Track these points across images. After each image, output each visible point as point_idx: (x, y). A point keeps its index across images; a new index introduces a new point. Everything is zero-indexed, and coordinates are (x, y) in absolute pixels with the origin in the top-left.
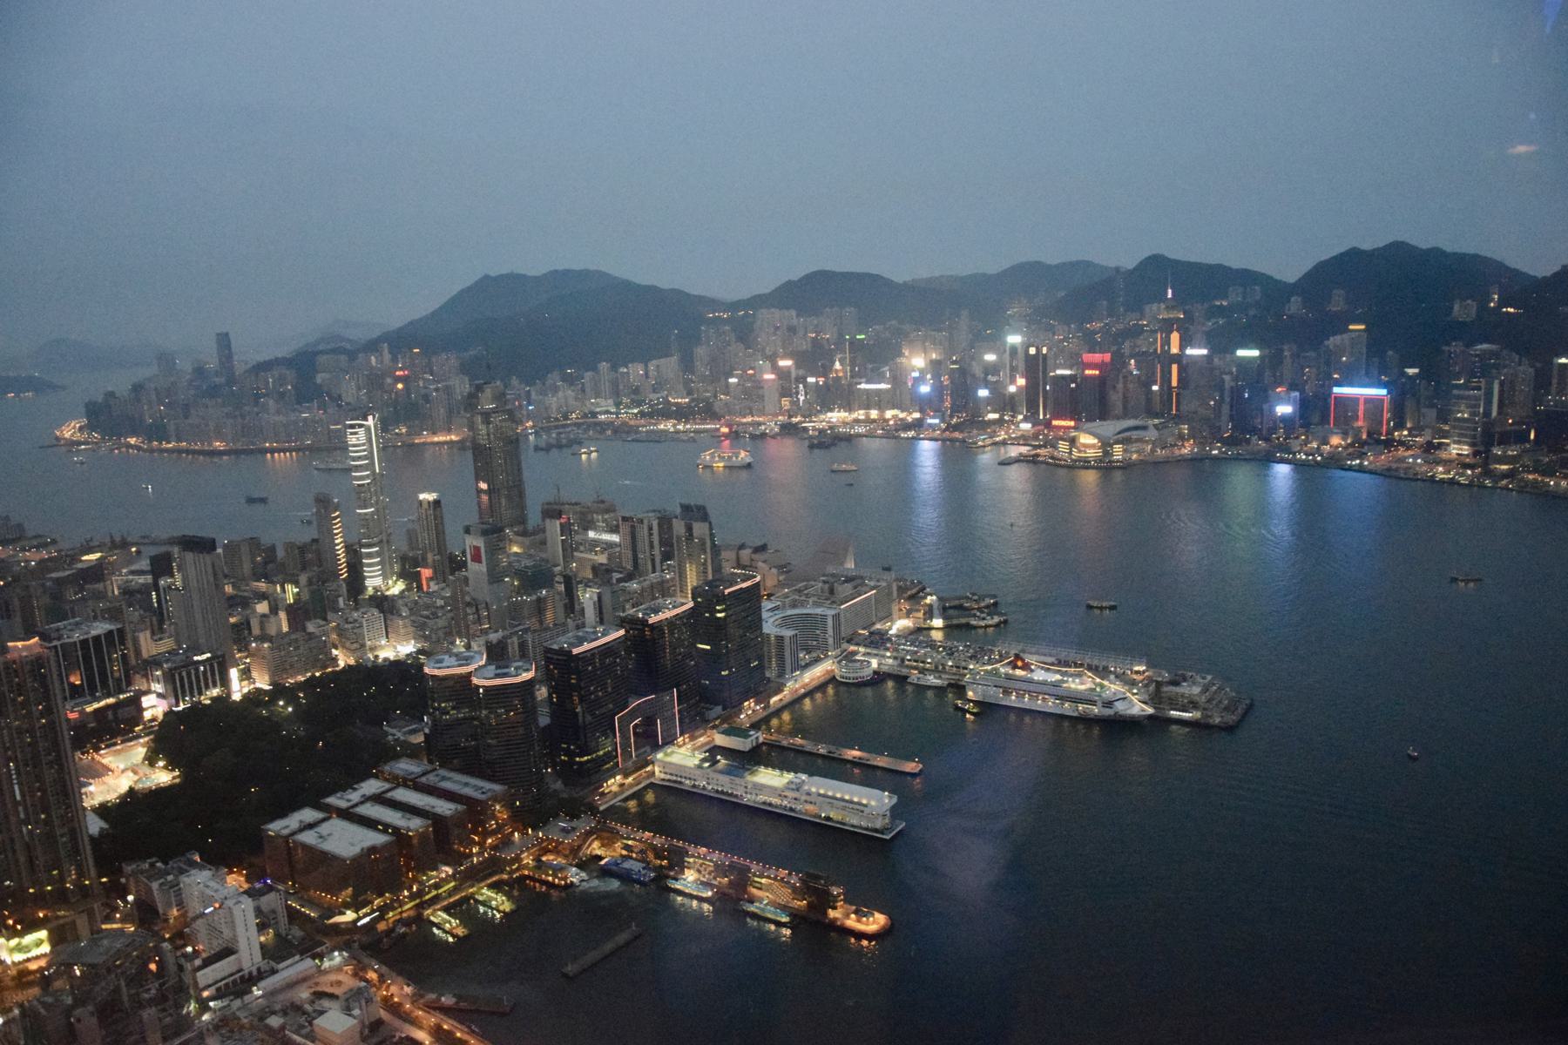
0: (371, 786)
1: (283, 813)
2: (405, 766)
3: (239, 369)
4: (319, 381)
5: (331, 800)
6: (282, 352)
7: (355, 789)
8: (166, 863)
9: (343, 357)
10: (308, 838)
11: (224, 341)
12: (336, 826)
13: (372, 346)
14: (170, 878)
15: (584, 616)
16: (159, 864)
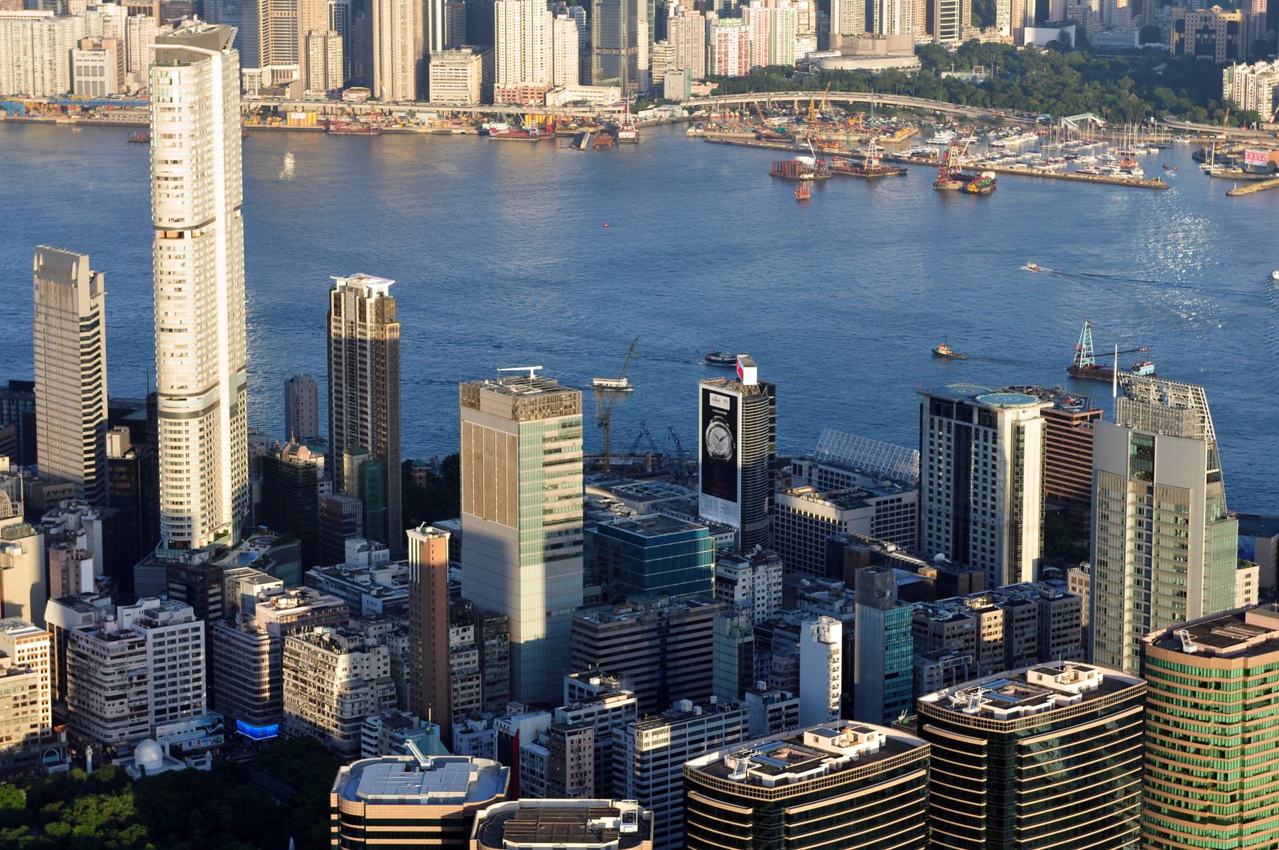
15: (796, 693)
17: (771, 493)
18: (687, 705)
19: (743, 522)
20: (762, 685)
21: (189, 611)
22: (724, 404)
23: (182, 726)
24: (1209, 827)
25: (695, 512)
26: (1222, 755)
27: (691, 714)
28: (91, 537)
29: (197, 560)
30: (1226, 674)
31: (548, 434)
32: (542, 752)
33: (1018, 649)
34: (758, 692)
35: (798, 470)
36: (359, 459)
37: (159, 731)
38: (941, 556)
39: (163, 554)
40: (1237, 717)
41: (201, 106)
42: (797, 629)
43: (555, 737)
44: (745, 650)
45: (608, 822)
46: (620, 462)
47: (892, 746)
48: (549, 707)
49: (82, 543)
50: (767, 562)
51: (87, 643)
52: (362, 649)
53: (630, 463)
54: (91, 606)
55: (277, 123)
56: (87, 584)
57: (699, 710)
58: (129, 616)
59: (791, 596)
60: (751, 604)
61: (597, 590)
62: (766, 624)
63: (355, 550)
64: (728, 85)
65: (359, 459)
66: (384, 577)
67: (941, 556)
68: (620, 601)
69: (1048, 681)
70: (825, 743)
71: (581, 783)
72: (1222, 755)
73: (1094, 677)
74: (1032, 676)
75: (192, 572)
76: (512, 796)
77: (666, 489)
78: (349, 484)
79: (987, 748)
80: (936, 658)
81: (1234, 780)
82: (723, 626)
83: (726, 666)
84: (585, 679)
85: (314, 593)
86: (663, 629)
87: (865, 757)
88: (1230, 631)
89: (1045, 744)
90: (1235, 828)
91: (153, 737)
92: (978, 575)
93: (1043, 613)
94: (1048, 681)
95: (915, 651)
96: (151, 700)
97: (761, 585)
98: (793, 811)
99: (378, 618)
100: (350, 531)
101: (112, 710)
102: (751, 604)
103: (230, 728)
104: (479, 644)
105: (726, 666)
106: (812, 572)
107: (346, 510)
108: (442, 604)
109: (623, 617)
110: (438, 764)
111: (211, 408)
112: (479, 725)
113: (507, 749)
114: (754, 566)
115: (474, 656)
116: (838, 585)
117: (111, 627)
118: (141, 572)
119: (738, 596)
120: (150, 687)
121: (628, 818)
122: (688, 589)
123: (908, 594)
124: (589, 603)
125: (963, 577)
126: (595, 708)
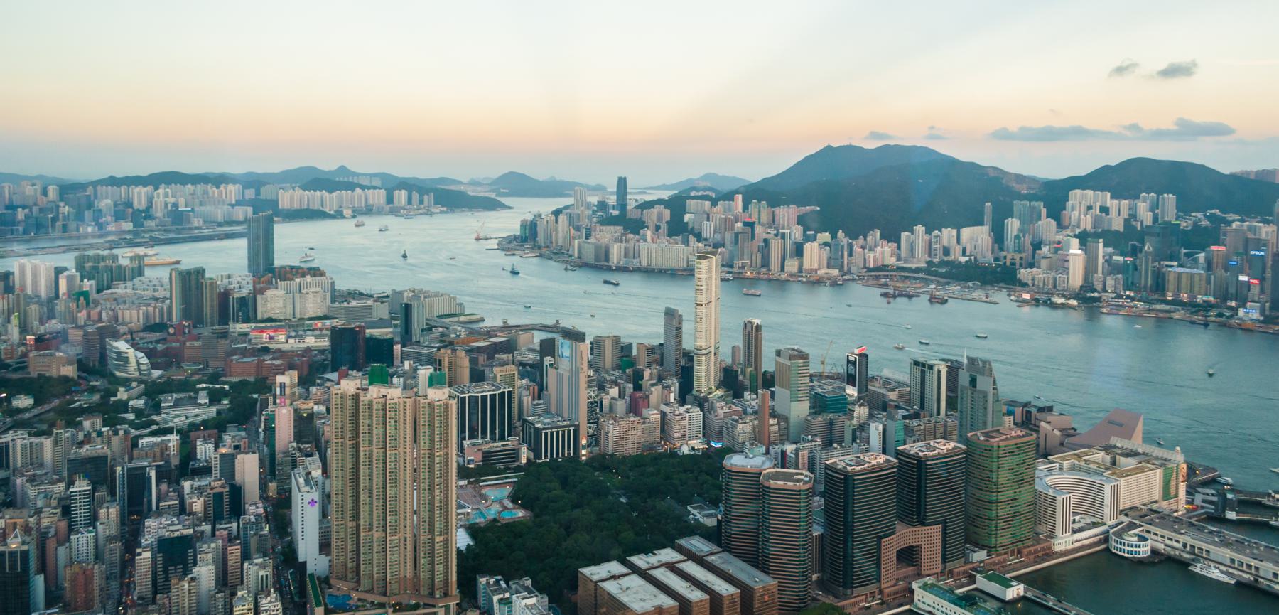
0: (668, 555)
1: (597, 560)
2: (697, 544)
3: (631, 205)
4: (685, 221)
5: (636, 560)
6: (665, 195)
7: (654, 554)
8: (507, 583)
9: (707, 204)
10: (611, 587)
11: (622, 183)
12: (635, 581)
13: (729, 196)
14: (507, 595)
15: (868, 444)
16: (502, 582)
18: (835, 445)
19: (858, 393)
20: (858, 441)
21: (699, 409)
22: (853, 359)
23: (695, 441)
24: (988, 493)
25: (844, 390)
26: (991, 471)
28: (675, 387)
29: (702, 395)
30: (992, 447)
32: (793, 456)
33: (938, 435)
35: (876, 380)
36: (749, 370)
37: (689, 442)
38: (915, 407)
39: (694, 393)
40: (995, 460)
41: (710, 269)
43: (797, 452)
44: (854, 431)
45: (800, 477)
47: (887, 461)
48: (796, 443)
49: (672, 389)
50: (864, 406)
51: (670, 416)
52: (745, 423)
54: (672, 406)
55: (741, 276)
56: (672, 400)
58: (682, 410)
59: (871, 416)
60: (859, 418)
61: (813, 410)
62: (864, 424)
63: (747, 395)
64: (870, 270)
65: (749, 370)
66: (754, 403)
67: (915, 407)
68: (819, 414)
69: (936, 445)
70: (867, 459)
72: (991, 471)
75: (701, 398)
76: (773, 468)
77: (838, 383)
78: (748, 376)
79: (917, 464)
80: (911, 437)
81: (995, 480)
82: (847, 423)
83: (848, 436)
84: (807, 436)
85: (733, 406)
86: (831, 423)
87: (878, 464)
88: (994, 434)
89: (936, 464)
90: (995, 494)
91: (687, 444)
92: (927, 413)
93: (945, 426)
94: (936, 445)
95: (905, 434)
96: (687, 433)
97: (862, 412)
98: (856, 478)
99: (750, 414)
100: (746, 389)
101: (676, 435)
102: (859, 418)
103: (708, 444)
104: (778, 424)
105: (848, 436)
106: (877, 409)
107: (746, 383)
108: (767, 412)
109: (820, 418)
110: (755, 456)
111: (710, 352)
114: (860, 406)
115: (777, 427)
117: (677, 413)
118: (689, 398)
119: (855, 414)
120: (687, 430)
121: (806, 476)
122: (840, 412)
124: (810, 414)
125: (922, 413)
126: (809, 444)
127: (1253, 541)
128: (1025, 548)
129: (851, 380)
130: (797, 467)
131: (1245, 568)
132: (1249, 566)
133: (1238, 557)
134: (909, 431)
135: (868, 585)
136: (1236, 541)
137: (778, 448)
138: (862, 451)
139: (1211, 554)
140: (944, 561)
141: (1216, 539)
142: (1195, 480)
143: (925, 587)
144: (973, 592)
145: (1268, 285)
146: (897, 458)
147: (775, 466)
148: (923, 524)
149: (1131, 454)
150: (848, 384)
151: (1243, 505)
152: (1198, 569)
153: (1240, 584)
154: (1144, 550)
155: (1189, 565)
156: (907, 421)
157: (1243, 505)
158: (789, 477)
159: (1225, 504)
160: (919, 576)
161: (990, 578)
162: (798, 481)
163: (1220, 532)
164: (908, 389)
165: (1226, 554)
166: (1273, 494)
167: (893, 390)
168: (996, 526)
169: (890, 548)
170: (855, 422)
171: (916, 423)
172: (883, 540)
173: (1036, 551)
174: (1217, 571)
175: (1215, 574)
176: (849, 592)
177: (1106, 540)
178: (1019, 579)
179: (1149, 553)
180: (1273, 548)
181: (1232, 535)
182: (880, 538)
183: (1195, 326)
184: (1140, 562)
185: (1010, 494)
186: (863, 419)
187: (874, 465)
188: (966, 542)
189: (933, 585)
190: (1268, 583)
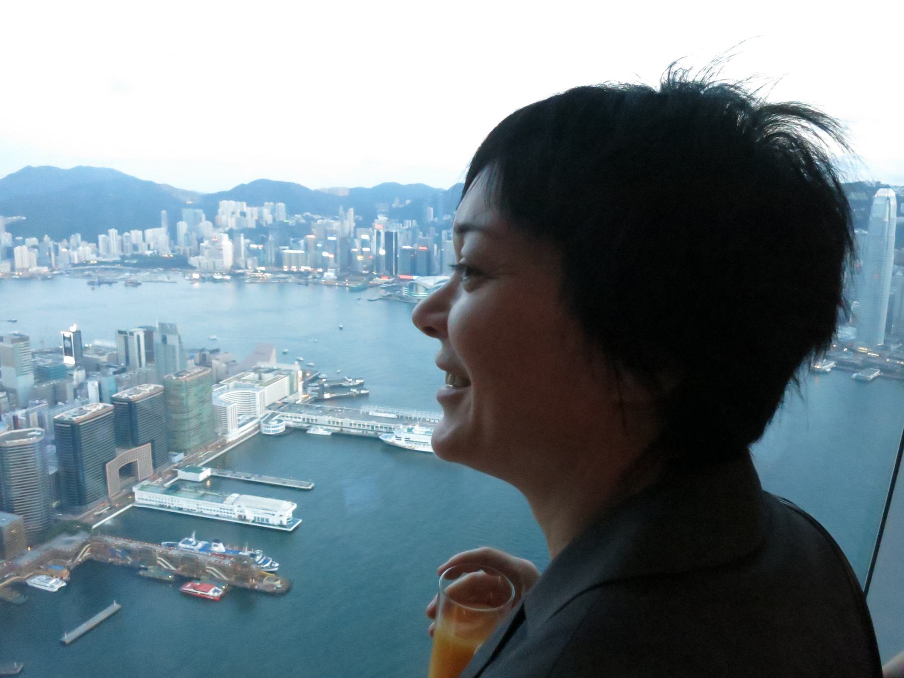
15: (87, 397)
17: (82, 356)
18: (60, 403)
20: (79, 397)
27: (61, 406)
30: (182, 382)
31: (22, 346)
32: (24, 418)
34: (78, 399)
38: (122, 364)
42: (87, 383)
43: (27, 415)
44: (75, 391)
46: (46, 350)
47: (105, 407)
48: (25, 408)
53: (49, 350)
57: (63, 404)
59: (88, 376)
61: (37, 380)
69: (141, 389)
70: (88, 409)
71: (34, 424)
73: (152, 387)
74: (138, 388)
83: (70, 394)
87: (98, 410)
94: (141, 389)
95: (117, 385)
102: (77, 379)
104: (7, 395)
109: (44, 385)
112: (8, 414)
113: (15, 419)
114: (78, 370)
115: (7, 399)
116: (99, 373)
119: (74, 377)
121: (38, 431)
123: (115, 373)
124: (36, 383)
127: (339, 408)
128: (209, 444)
129: (68, 352)
130: (28, 426)
131: (336, 425)
132: (334, 422)
133: (331, 418)
134: (119, 382)
135: (98, 498)
136: (331, 410)
137: (10, 415)
138: (83, 404)
139: (344, 424)
140: (155, 466)
141: (320, 412)
142: (307, 379)
143: (143, 488)
144: (178, 482)
145: (338, 256)
146: (113, 404)
147: (9, 429)
148: (137, 445)
149: (270, 371)
150: (66, 355)
151: (333, 388)
152: (311, 431)
153: (335, 435)
154: (281, 429)
155: (307, 430)
156: (117, 375)
157: (333, 388)
158: (23, 435)
159: (323, 390)
160: (137, 482)
161: (187, 470)
162: (32, 436)
163: (322, 407)
164: (115, 352)
165: (326, 419)
166: (347, 379)
167: (103, 354)
168: (189, 435)
169: (113, 468)
170: (75, 383)
171: (124, 376)
172: (107, 465)
173: (217, 445)
174: (322, 429)
175: (321, 431)
176: (84, 507)
177: (259, 427)
178: (207, 465)
179: (284, 429)
180: (349, 410)
181: (328, 406)
182: (106, 463)
183: (301, 285)
184: (279, 436)
185: (195, 412)
186: (81, 380)
187: (94, 412)
188: (169, 451)
189: (148, 485)
190: (347, 430)
